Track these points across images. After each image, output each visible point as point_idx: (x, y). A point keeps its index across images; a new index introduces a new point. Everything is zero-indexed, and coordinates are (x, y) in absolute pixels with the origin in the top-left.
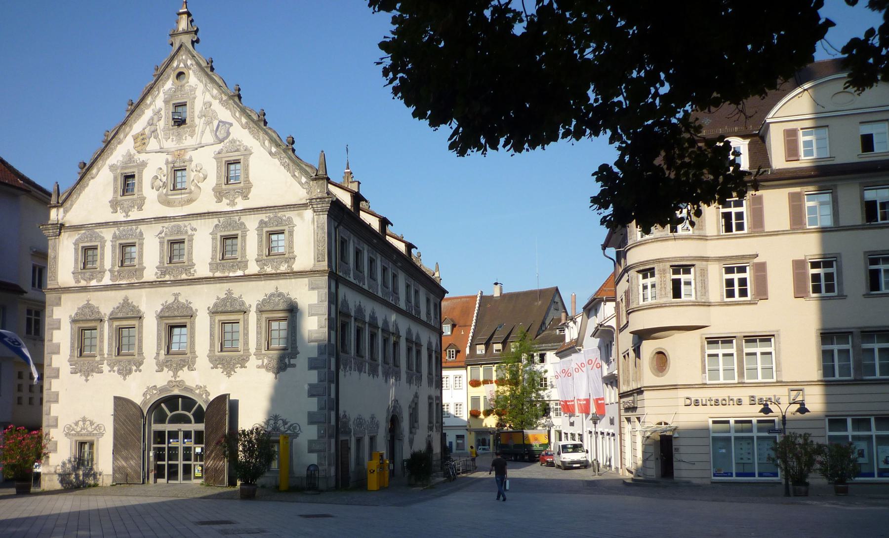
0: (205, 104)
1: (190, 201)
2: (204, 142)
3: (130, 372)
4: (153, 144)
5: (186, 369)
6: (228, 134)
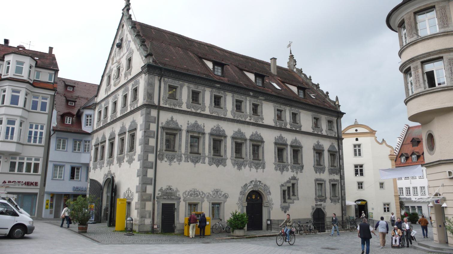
3: (102, 168)
4: (115, 61)
5: (112, 164)
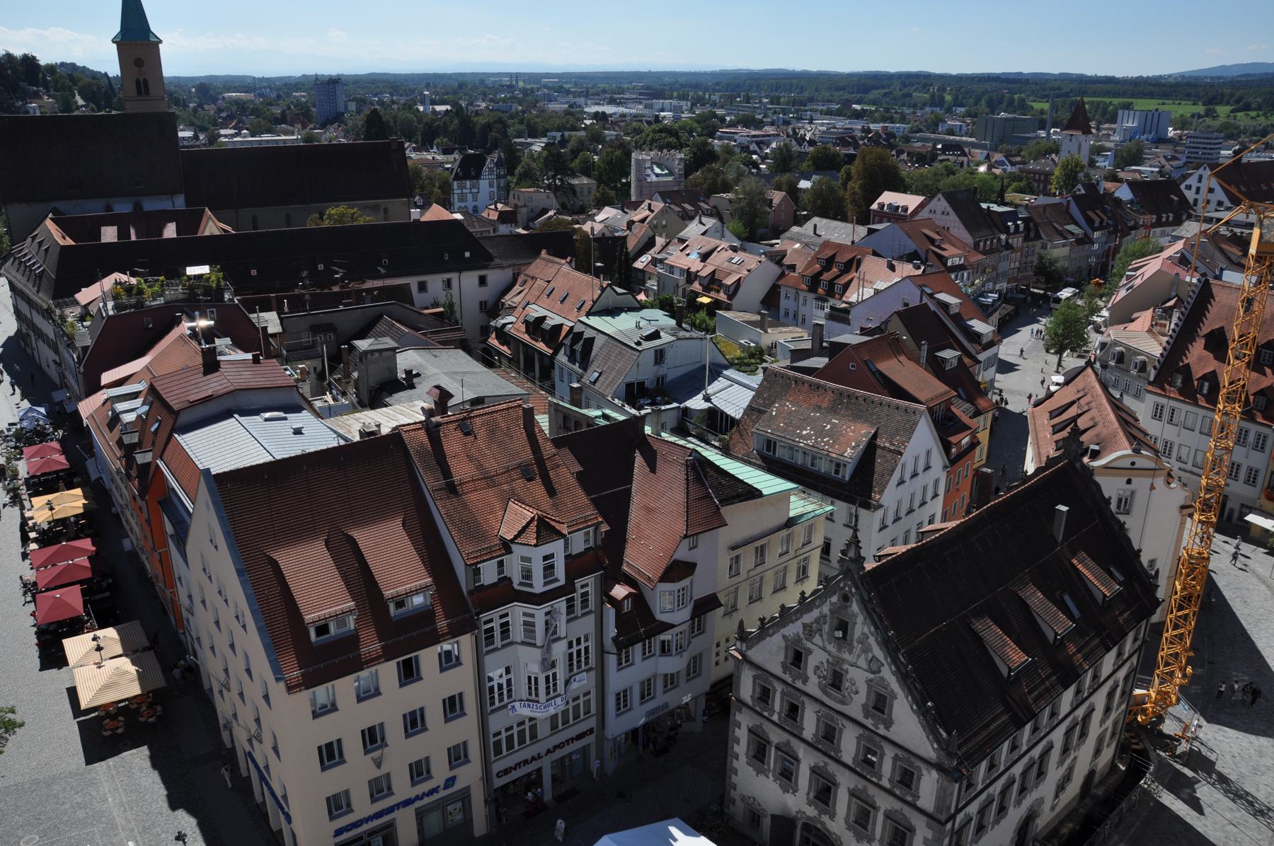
0: (863, 634)
1: (843, 703)
2: (859, 664)
4: (817, 639)
6: (879, 671)
